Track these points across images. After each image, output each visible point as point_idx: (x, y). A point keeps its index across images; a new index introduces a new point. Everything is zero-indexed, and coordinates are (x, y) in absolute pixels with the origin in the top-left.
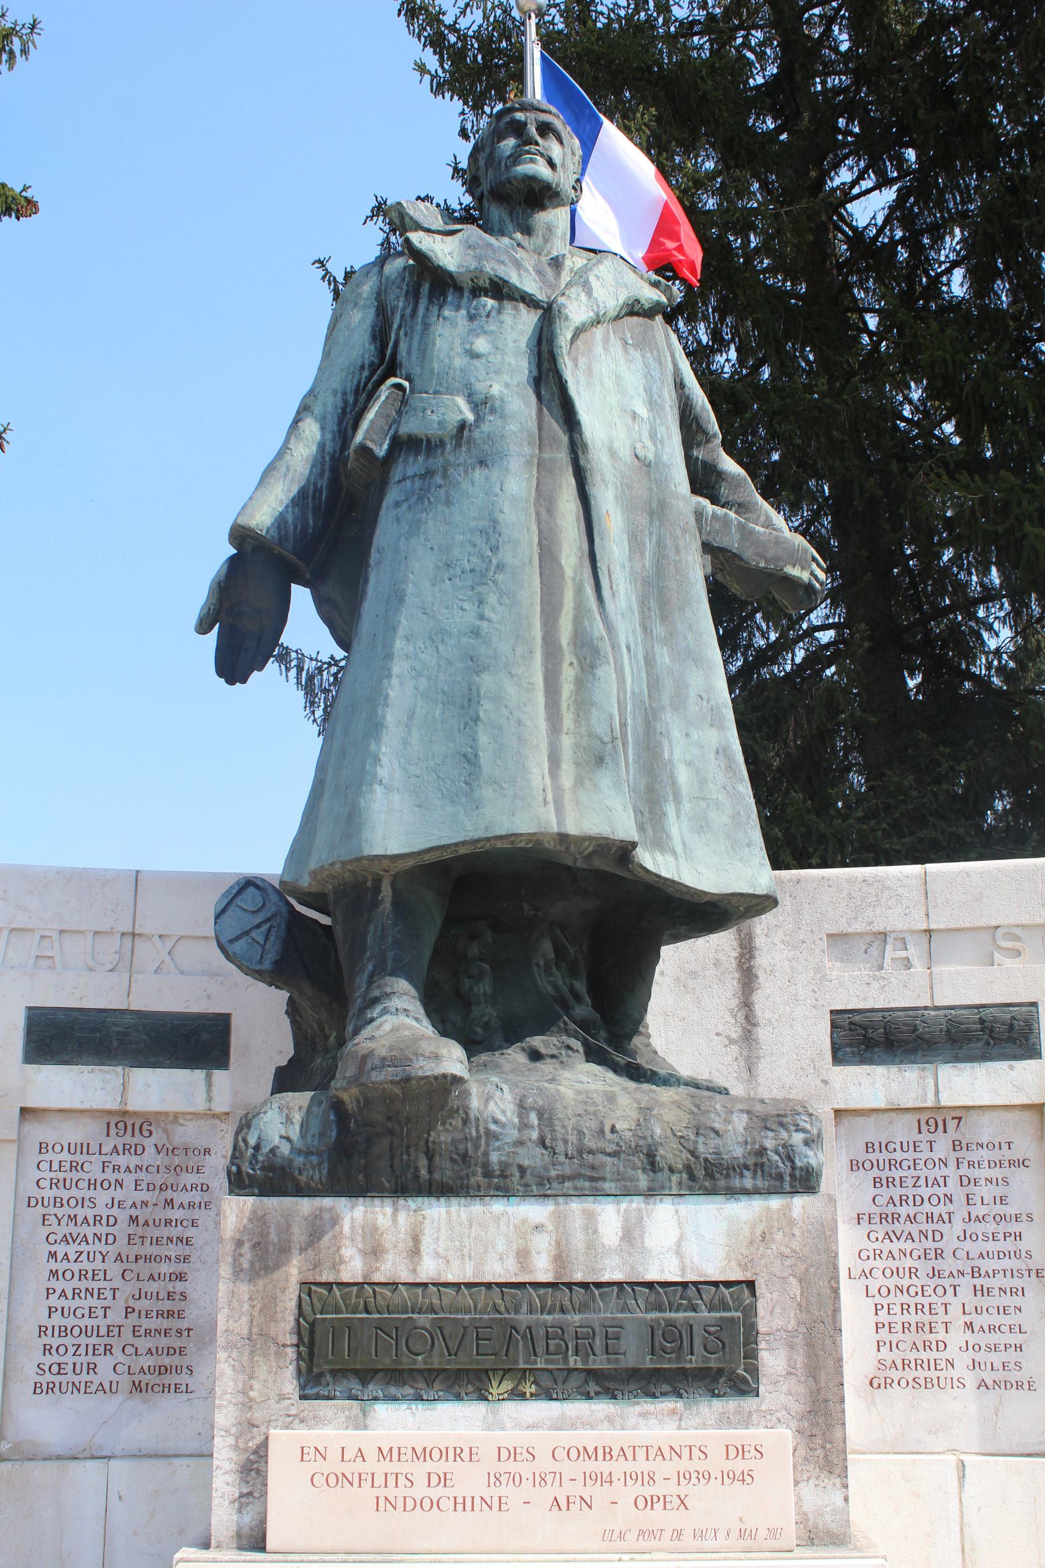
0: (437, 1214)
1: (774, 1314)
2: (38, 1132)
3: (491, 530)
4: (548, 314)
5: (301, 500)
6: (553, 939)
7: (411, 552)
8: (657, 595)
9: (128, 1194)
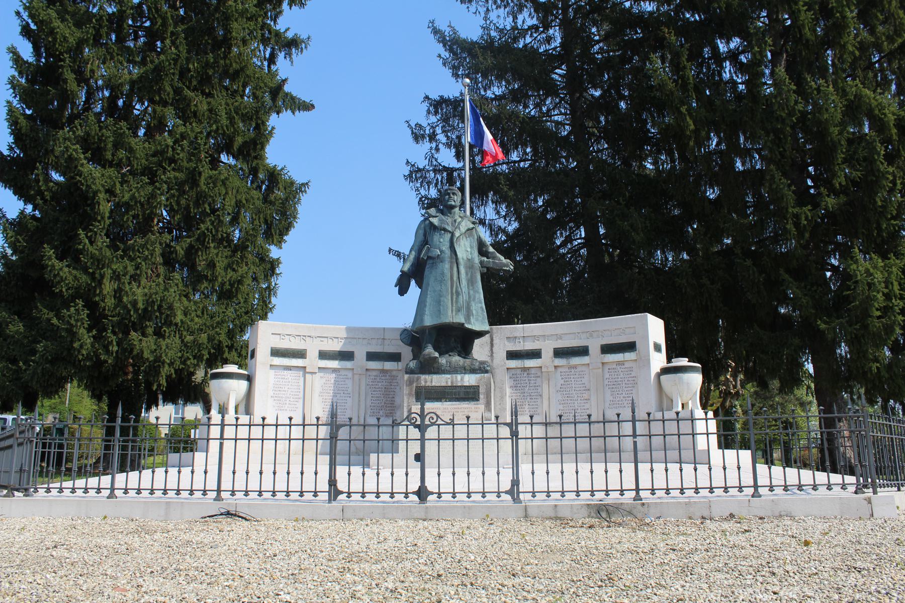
0: (435, 376)
1: (482, 390)
2: (369, 373)
3: (443, 274)
4: (453, 234)
5: (412, 265)
6: (458, 339)
7: (430, 276)
8: (471, 282)
9: (384, 383)
